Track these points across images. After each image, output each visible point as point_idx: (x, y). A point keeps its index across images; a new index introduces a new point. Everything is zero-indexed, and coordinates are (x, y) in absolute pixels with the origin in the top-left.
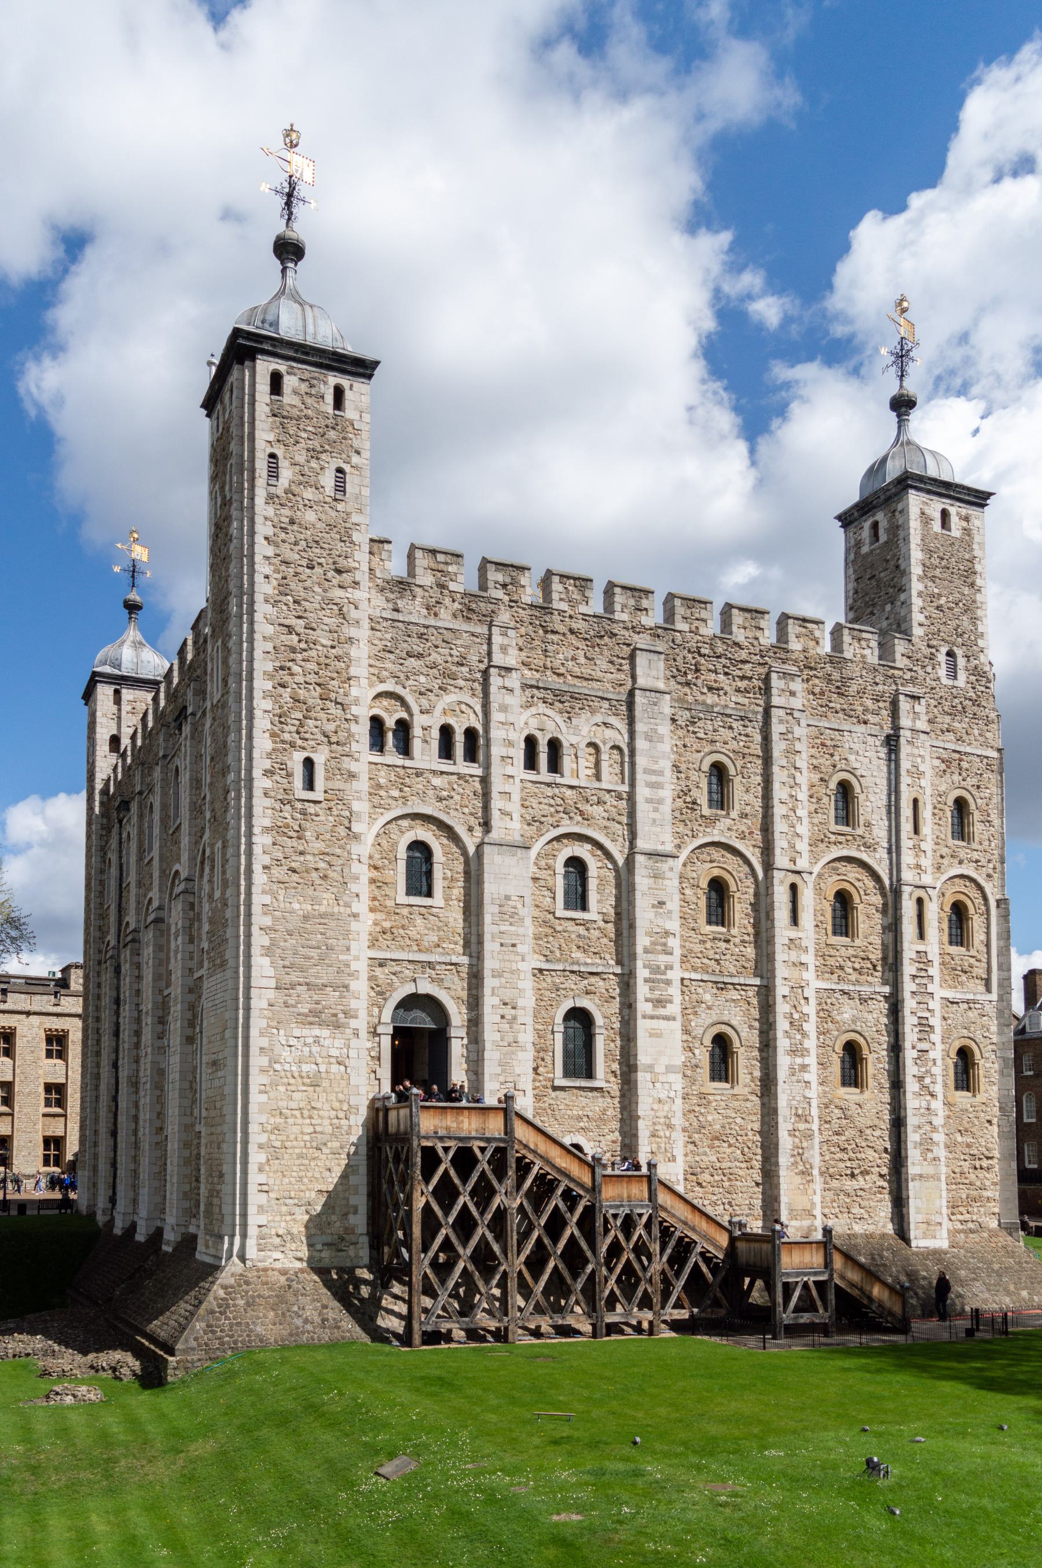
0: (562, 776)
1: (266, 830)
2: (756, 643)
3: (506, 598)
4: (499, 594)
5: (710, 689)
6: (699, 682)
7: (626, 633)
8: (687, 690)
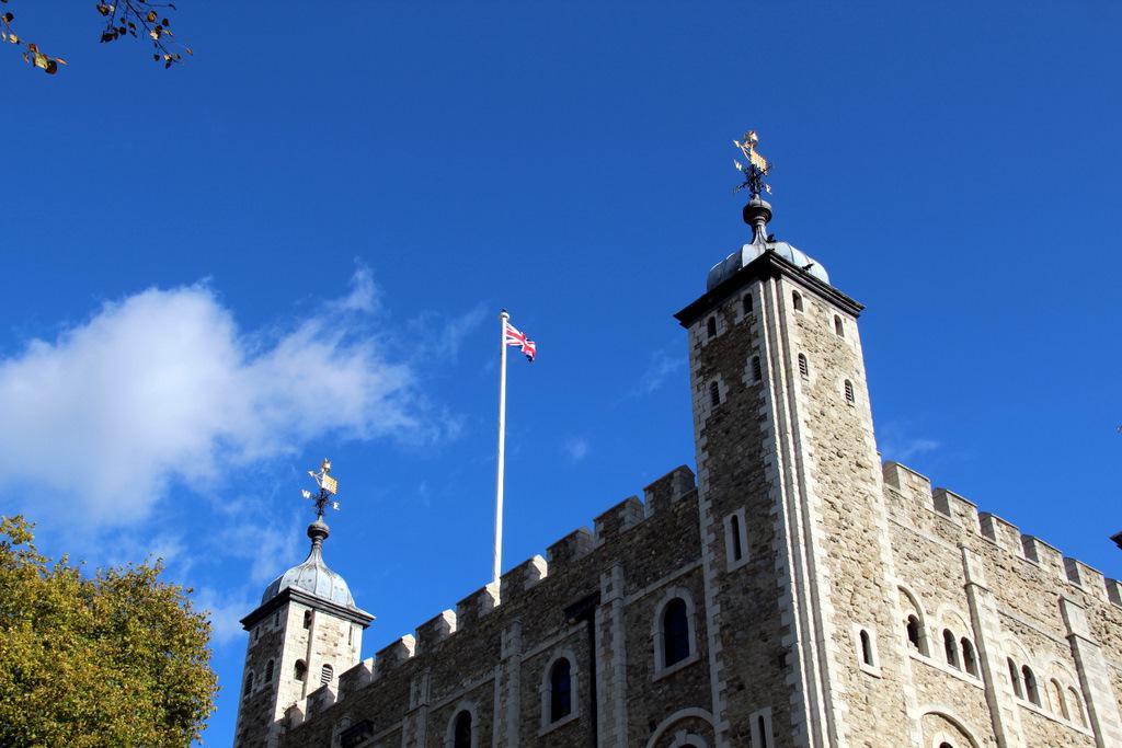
0: (1040, 706)
1: (843, 696)
3: (964, 527)
4: (958, 521)
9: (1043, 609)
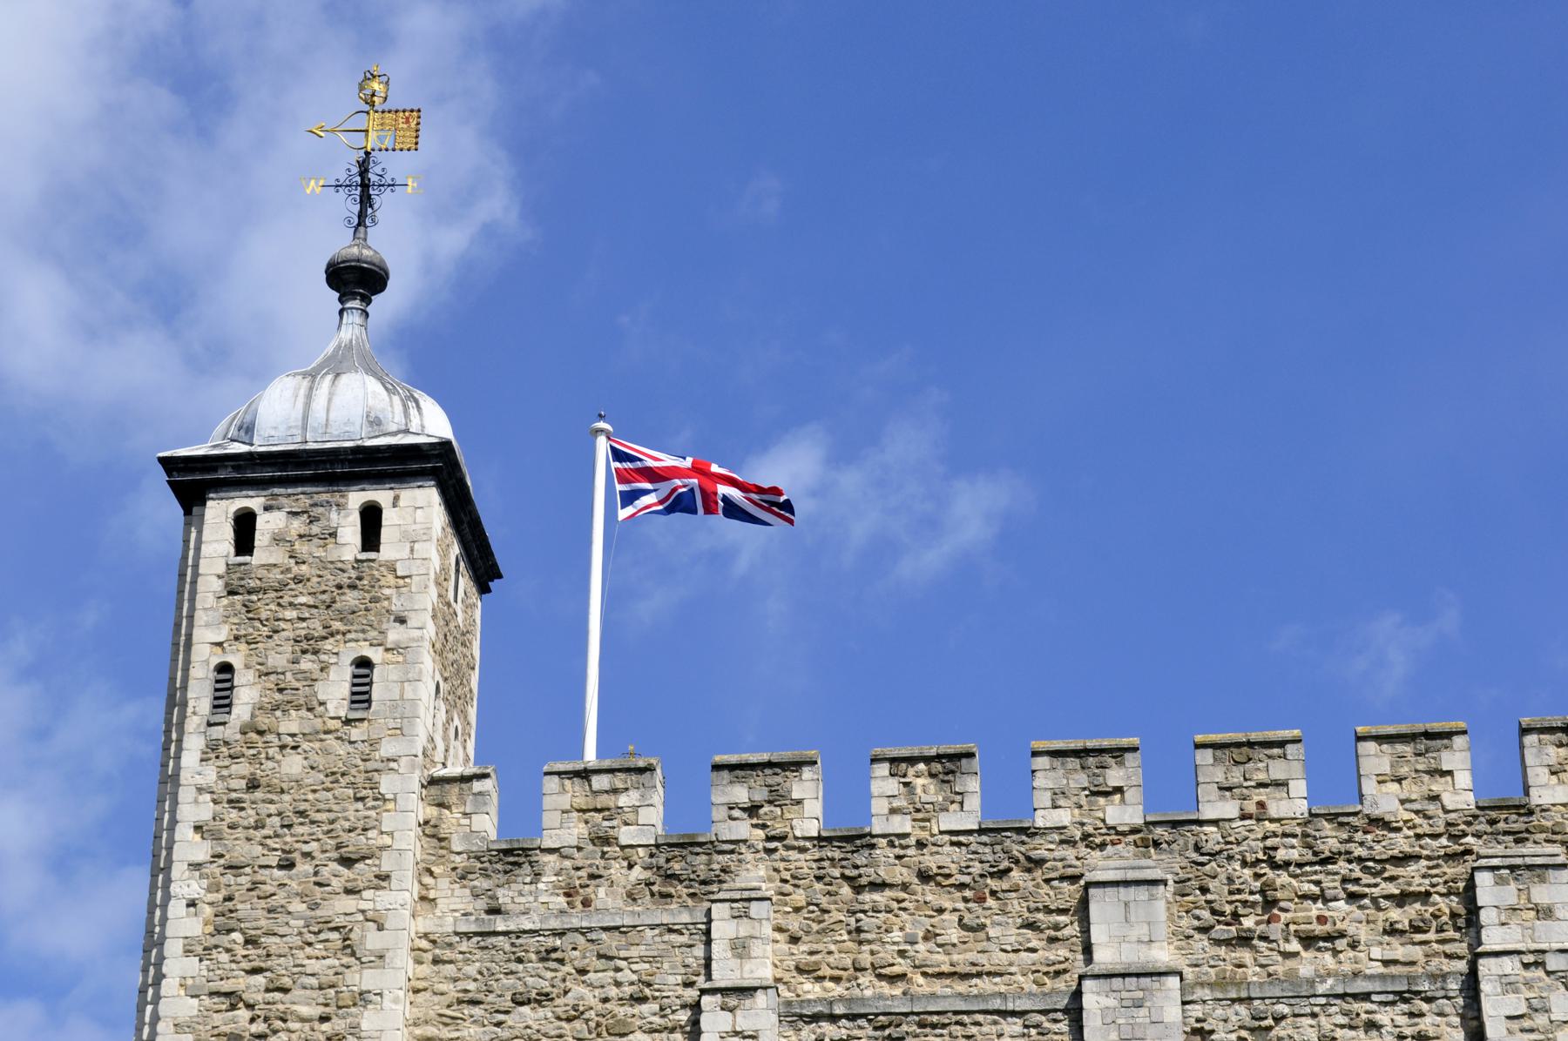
2: (1432, 808)
3: (761, 833)
4: (743, 829)
5: (1308, 941)
6: (1275, 931)
7: (1069, 853)
8: (1245, 955)
9: (1012, 936)
